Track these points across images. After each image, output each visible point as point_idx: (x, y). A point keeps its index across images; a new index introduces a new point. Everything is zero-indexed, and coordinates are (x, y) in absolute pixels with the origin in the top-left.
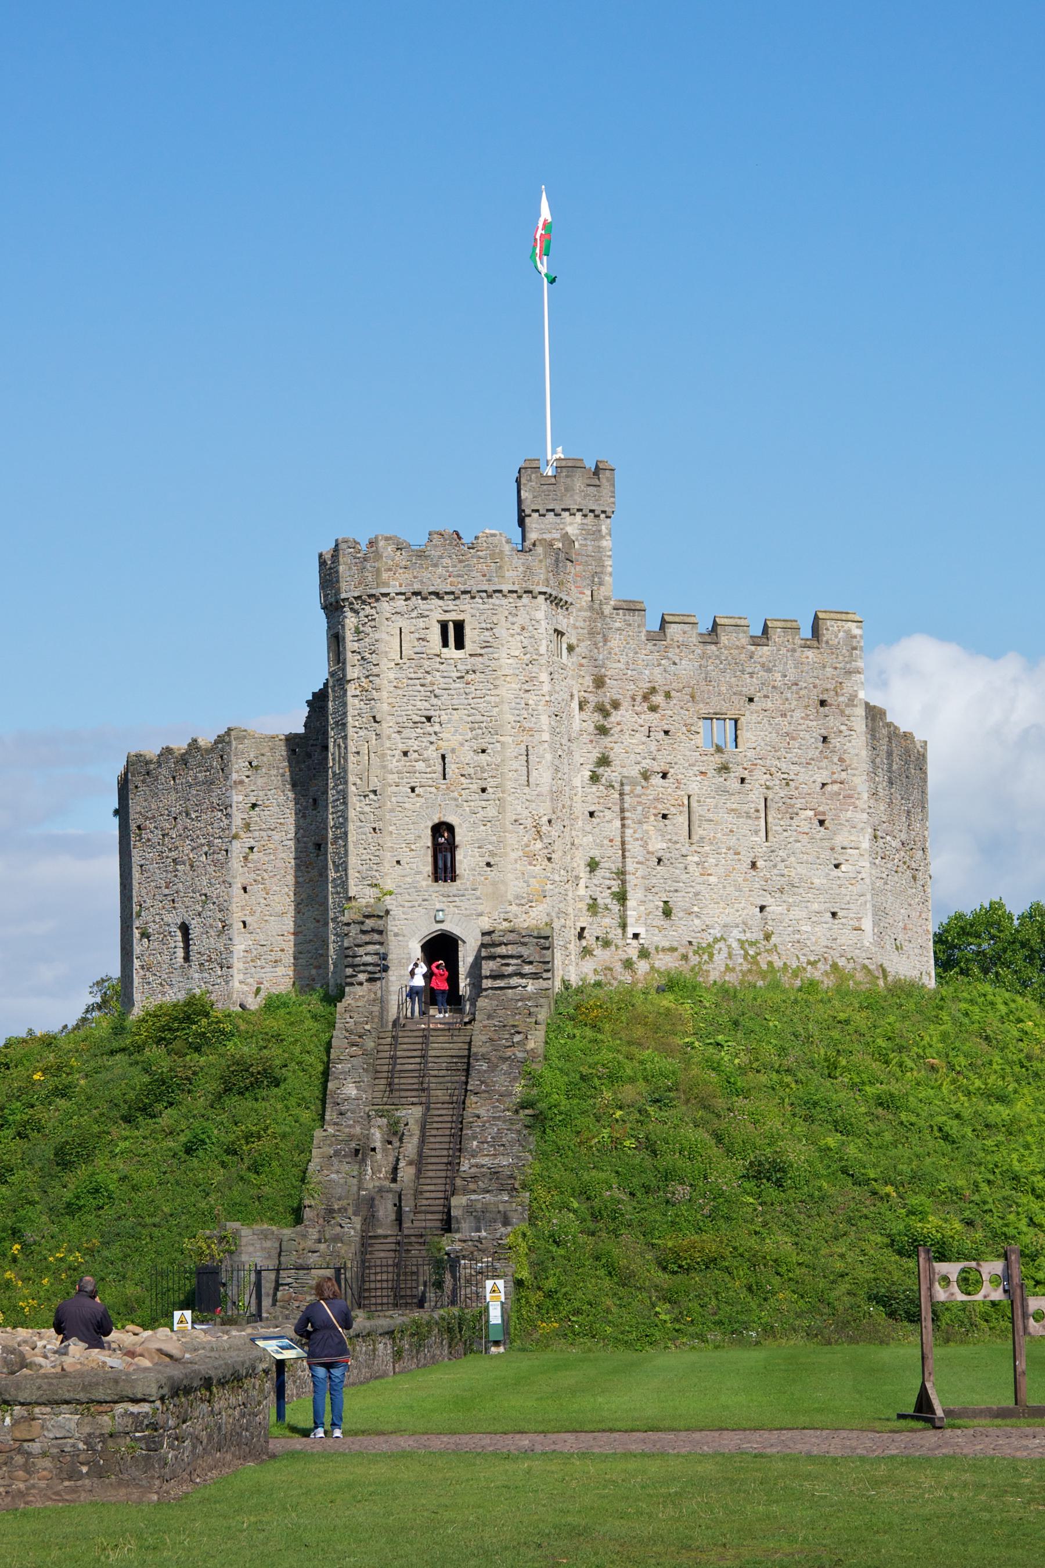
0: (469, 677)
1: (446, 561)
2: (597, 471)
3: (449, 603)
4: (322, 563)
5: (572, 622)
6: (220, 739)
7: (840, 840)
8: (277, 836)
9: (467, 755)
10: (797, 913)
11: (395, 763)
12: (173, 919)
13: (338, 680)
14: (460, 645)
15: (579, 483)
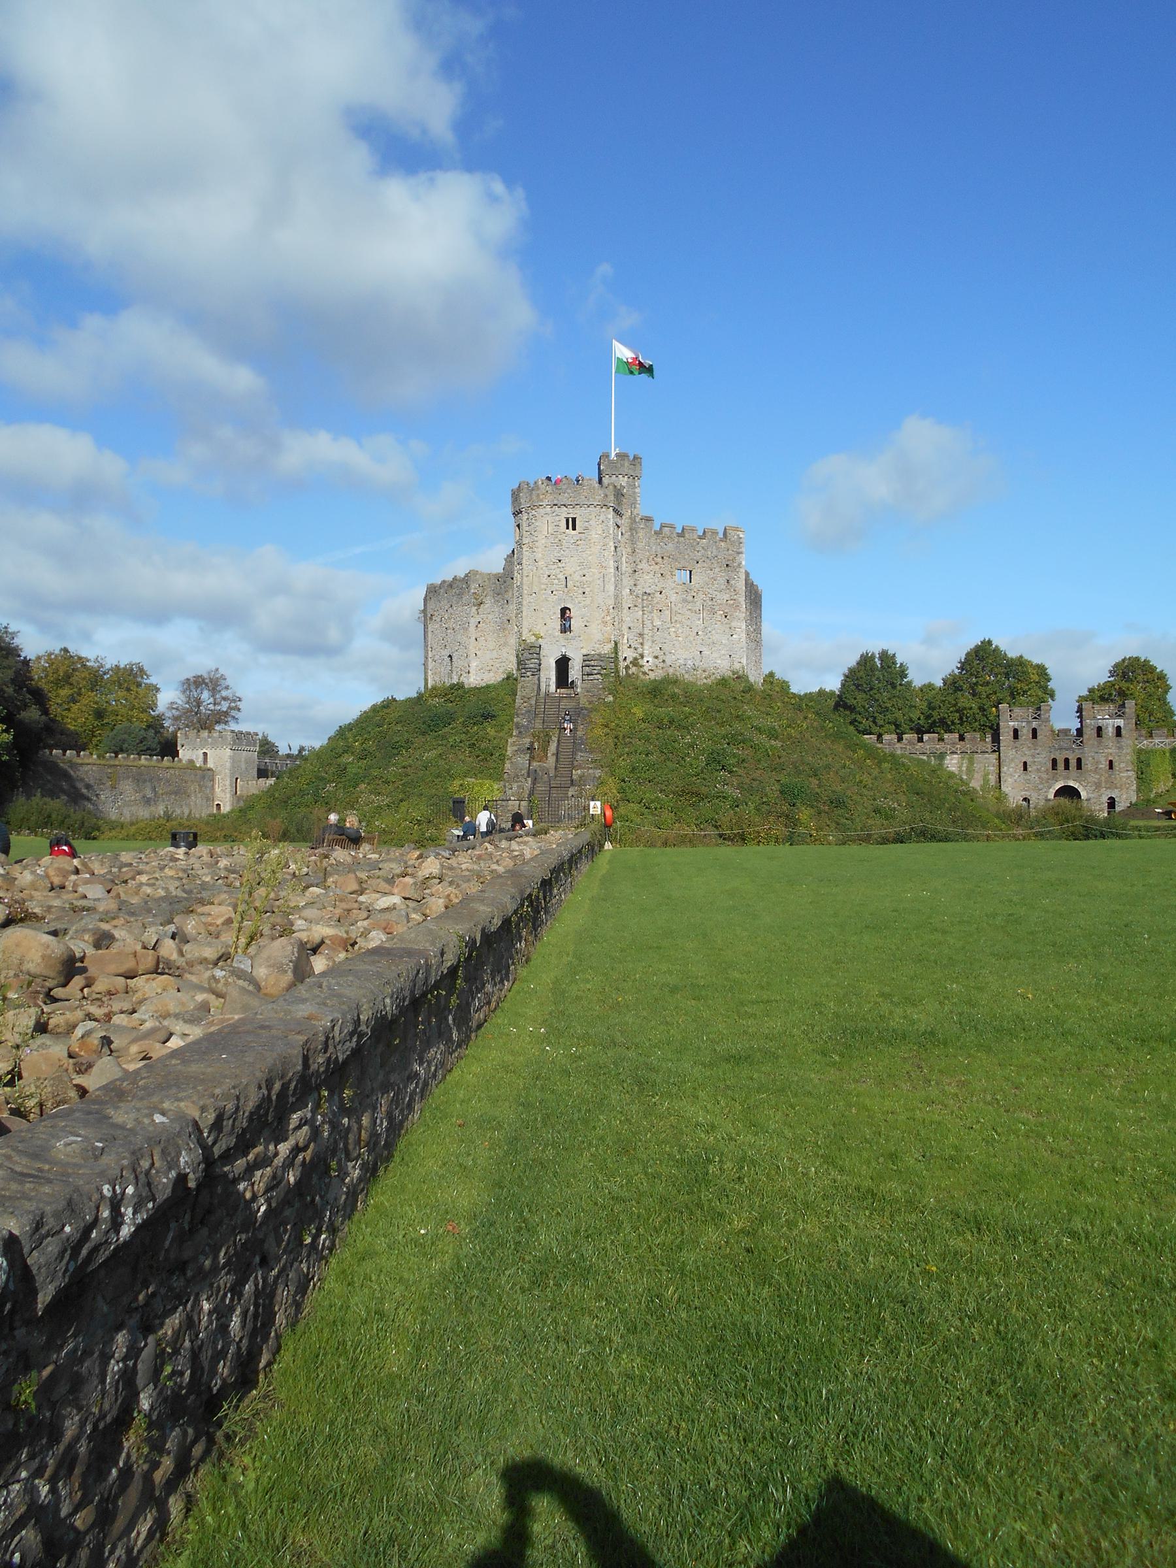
0: (579, 542)
1: (569, 491)
2: (635, 458)
3: (571, 510)
4: (513, 494)
5: (624, 522)
6: (467, 575)
7: (734, 624)
8: (490, 617)
9: (577, 577)
10: (715, 655)
11: (545, 580)
12: (446, 653)
13: (520, 544)
14: (574, 529)
15: (626, 464)
